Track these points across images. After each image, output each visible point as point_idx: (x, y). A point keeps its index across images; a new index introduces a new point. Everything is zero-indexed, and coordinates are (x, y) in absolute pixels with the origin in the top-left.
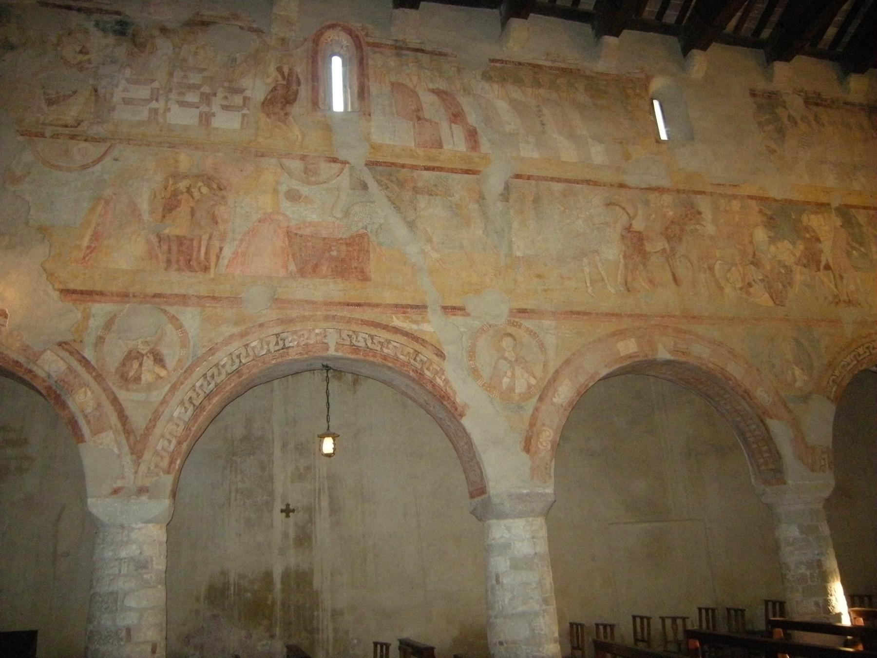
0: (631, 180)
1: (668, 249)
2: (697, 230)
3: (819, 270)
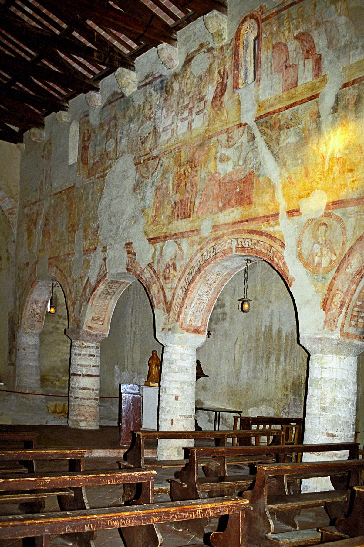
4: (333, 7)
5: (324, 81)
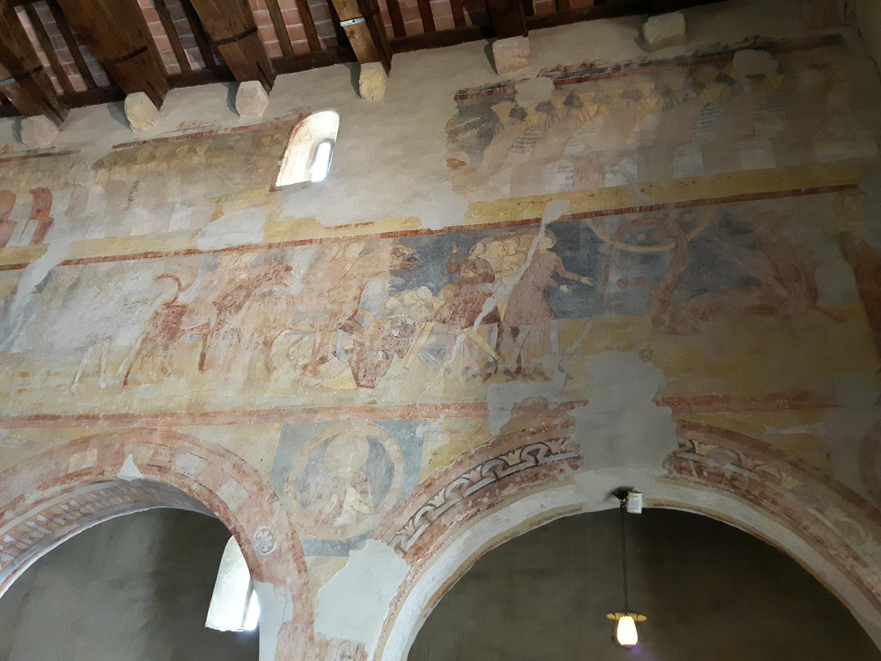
0: (203, 244)
1: (213, 324)
2: (271, 292)
3: (471, 323)
4: (93, 172)
5: (44, 251)
